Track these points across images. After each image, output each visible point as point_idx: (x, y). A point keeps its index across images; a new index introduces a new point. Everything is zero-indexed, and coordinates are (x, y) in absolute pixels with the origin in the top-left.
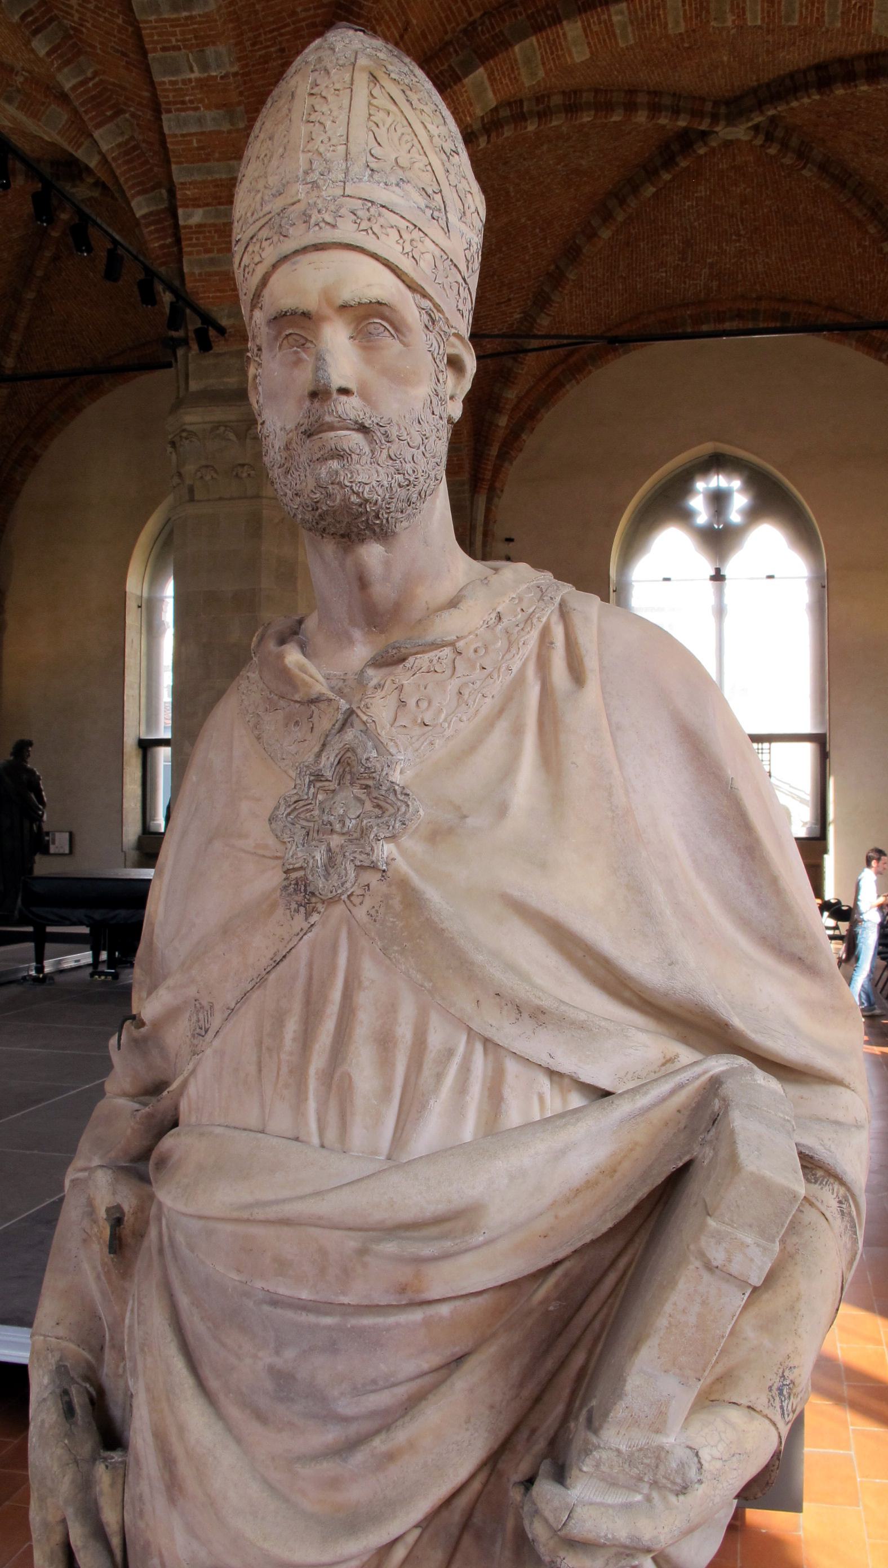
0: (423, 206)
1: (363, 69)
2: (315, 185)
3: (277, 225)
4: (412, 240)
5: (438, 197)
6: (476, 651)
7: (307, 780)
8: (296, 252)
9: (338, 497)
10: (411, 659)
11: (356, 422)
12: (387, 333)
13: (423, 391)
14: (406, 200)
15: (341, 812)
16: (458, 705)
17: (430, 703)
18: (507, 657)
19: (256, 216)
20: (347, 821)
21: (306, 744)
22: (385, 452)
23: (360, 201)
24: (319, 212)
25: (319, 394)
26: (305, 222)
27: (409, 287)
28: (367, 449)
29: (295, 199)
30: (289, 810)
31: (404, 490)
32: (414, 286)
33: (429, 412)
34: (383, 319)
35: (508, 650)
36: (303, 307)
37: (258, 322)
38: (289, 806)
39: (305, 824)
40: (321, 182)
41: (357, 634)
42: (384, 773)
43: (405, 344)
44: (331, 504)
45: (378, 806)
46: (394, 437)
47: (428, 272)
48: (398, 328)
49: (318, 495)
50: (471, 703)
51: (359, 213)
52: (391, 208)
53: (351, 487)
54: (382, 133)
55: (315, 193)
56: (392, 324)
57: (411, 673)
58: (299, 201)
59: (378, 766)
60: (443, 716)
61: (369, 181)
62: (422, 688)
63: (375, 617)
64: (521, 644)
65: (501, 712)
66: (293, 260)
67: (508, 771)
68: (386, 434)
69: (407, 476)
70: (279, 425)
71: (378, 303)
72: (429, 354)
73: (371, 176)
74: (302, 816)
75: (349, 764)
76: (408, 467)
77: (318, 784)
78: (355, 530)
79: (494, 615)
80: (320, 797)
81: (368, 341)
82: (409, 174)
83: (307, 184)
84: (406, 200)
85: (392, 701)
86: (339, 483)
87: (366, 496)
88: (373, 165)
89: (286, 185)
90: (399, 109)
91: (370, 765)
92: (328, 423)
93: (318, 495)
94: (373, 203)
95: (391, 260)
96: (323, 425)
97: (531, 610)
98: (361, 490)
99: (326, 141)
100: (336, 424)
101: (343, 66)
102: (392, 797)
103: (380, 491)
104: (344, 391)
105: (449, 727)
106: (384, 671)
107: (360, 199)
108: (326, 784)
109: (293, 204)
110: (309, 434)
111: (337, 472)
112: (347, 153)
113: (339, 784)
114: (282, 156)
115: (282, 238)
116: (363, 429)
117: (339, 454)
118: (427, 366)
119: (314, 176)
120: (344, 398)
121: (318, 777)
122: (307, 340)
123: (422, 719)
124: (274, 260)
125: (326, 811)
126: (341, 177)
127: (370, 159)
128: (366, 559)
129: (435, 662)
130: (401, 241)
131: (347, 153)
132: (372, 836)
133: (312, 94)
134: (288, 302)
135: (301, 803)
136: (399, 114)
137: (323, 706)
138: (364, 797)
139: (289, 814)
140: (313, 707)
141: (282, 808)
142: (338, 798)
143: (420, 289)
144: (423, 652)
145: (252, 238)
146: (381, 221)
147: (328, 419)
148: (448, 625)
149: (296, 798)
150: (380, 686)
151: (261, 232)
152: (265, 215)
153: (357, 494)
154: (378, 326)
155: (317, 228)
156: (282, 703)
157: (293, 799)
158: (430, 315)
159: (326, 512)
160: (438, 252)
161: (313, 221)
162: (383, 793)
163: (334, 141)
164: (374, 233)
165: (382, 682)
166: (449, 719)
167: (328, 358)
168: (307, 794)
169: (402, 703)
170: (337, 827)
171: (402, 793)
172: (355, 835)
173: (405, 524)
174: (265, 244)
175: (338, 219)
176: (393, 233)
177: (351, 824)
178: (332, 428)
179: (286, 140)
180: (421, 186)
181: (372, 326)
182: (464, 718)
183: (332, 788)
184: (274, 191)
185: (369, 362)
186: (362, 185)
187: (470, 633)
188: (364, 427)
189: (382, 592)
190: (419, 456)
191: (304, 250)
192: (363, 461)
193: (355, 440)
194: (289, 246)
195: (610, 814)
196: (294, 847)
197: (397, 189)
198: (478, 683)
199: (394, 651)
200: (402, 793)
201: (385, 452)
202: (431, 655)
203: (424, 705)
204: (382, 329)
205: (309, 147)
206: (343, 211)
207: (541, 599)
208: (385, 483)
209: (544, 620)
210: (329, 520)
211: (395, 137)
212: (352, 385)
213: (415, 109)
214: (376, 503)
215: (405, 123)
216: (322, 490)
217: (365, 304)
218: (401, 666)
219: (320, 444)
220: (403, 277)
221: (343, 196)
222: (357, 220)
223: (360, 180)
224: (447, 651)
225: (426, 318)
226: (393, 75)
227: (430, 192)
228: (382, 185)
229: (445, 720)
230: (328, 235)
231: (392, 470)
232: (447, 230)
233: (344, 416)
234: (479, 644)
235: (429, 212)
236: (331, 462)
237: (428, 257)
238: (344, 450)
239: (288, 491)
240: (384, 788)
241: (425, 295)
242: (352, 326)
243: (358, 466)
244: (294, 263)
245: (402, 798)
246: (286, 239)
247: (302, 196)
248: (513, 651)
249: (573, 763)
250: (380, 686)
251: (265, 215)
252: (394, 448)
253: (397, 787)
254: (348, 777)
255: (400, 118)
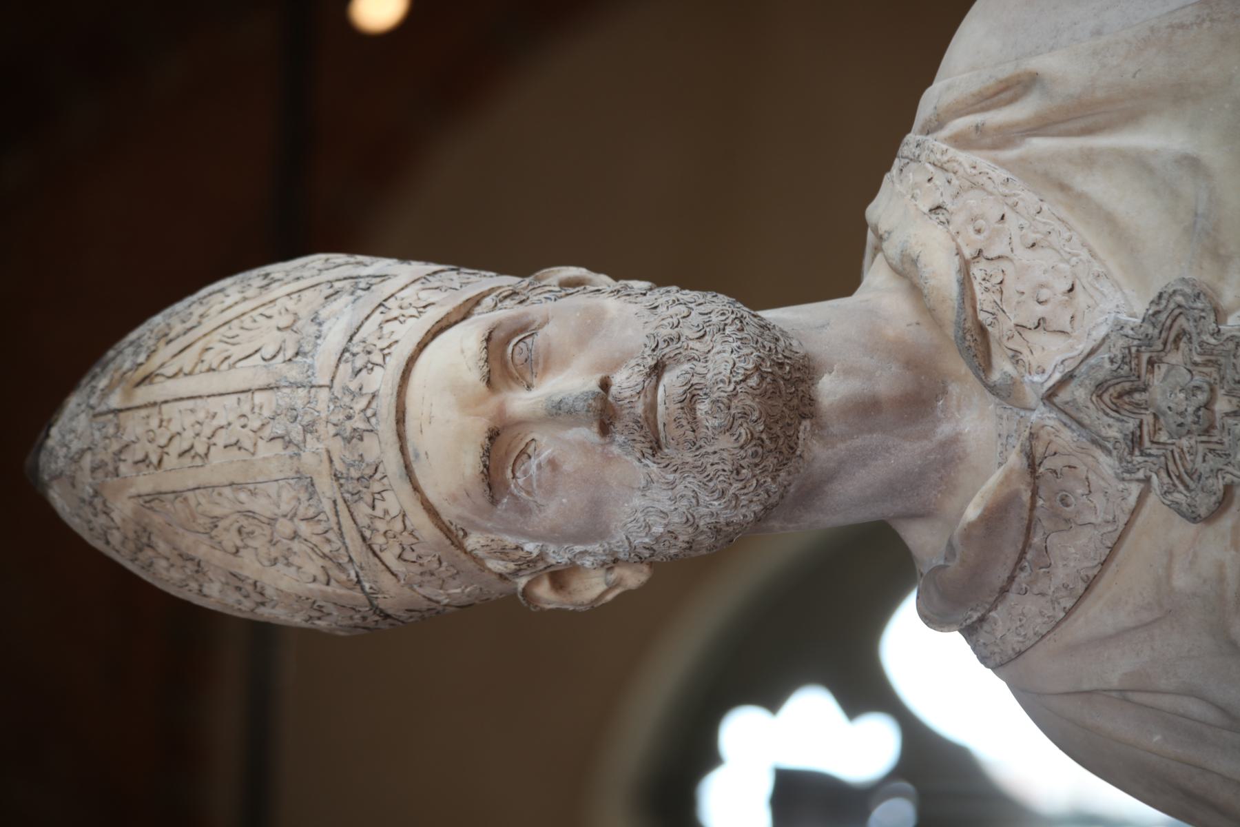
0: (352, 298)
1: (128, 395)
2: (308, 429)
3: (358, 482)
4: (401, 308)
5: (337, 285)
6: (979, 231)
7: (1140, 459)
8: (403, 450)
9: (749, 402)
10: (982, 316)
11: (649, 375)
12: (527, 340)
13: (612, 305)
14: (340, 318)
15: (1182, 396)
16: (1051, 247)
17: (1042, 286)
18: (990, 186)
19: (331, 535)
20: (1194, 383)
21: (1092, 477)
22: (691, 344)
23: (341, 366)
24: (349, 418)
25: (604, 413)
26: (361, 439)
27: (464, 319)
28: (686, 366)
29: (325, 457)
30: (1181, 488)
31: (746, 328)
32: (464, 311)
33: (641, 298)
34: (508, 343)
35: (982, 187)
36: (482, 438)
37: (483, 542)
38: (1174, 485)
39: (1199, 459)
40: (307, 419)
41: (945, 430)
42: (1131, 332)
43: (546, 322)
44: (757, 414)
45: (1177, 339)
46: (674, 332)
47: (444, 295)
48: (523, 329)
49: (743, 431)
50: (1048, 228)
51: (359, 362)
52: (353, 330)
53: (737, 383)
54: (237, 352)
55: (321, 428)
56: (516, 333)
57: (1000, 316)
58: (328, 452)
59: (1121, 342)
60: (1062, 266)
61: (312, 357)
62: (1023, 297)
63: (919, 401)
64: (974, 171)
65: (1063, 188)
66: (412, 458)
67: (1140, 164)
68: (669, 341)
69: (729, 321)
70: (638, 502)
71: (488, 339)
72: (559, 301)
73: (305, 354)
74: (1189, 466)
75: (1120, 396)
76: (715, 319)
77: (1147, 443)
78: (795, 402)
79: (934, 216)
80: (1163, 437)
81: (537, 364)
82: (305, 313)
83: (305, 441)
84: (340, 318)
85: (1038, 338)
86: (730, 398)
87: (751, 366)
88: (290, 353)
89: (299, 476)
90: (199, 339)
91: (1120, 356)
92: (645, 411)
93: (743, 431)
94: (345, 350)
95: (428, 327)
96: (647, 419)
97: (931, 168)
98: (742, 371)
99: (243, 421)
100: (648, 400)
101: (118, 427)
102: (1163, 317)
103: (745, 351)
104: (605, 385)
105: (1077, 255)
106: (994, 347)
107: (337, 366)
108: (1145, 429)
109: (331, 461)
110: (656, 447)
111: (713, 402)
112: (268, 388)
113: (1146, 409)
114: (253, 493)
115: (378, 476)
116: (658, 370)
117: (690, 398)
118: (579, 300)
119: (296, 432)
120: (614, 390)
121: (1135, 441)
122: (523, 452)
123: (1064, 294)
124: (408, 487)
125: (1180, 420)
126: (302, 392)
127: (280, 358)
128: (838, 396)
129: (988, 285)
130: (402, 319)
131: (268, 388)
132: (1212, 341)
133: (160, 461)
134: (471, 462)
135: (1172, 467)
136: (208, 338)
137: (1039, 450)
138: (1164, 368)
139: (1187, 487)
140: (1041, 470)
141: (1177, 497)
142: (1164, 406)
143: (469, 305)
144: (973, 299)
145: (364, 539)
146: (372, 339)
147: (640, 409)
148: (941, 271)
149: (1163, 474)
150: (1015, 357)
151: (359, 521)
152: (337, 515)
153: (746, 378)
154: (517, 349)
155: (373, 420)
156: (1037, 540)
157: (1166, 480)
158: (506, 297)
159: (768, 428)
160: (418, 286)
161: (362, 425)
162: (1157, 331)
163: (246, 408)
164: (389, 347)
165: (1011, 353)
166: (1067, 257)
167: (557, 399)
168: (1157, 456)
169: (1040, 324)
170: (1202, 397)
171: (1158, 304)
172: (1215, 375)
173: (795, 343)
174: (379, 512)
175: (364, 391)
176: (388, 327)
177: (1198, 380)
178: (652, 407)
179: (227, 491)
180: (323, 300)
181: (517, 357)
182: (1067, 235)
183: (1150, 419)
184: (304, 496)
185: (565, 363)
186: (317, 364)
187: (954, 240)
188: (656, 366)
189: (887, 381)
190: (703, 309)
191: (401, 436)
192: (704, 371)
193: (672, 381)
194: (392, 463)
195: (1207, 25)
196: (1230, 469)
197: (325, 328)
198: (1022, 221)
199: (968, 337)
200: (1158, 304)
201: (691, 344)
202: (978, 289)
203: (1044, 294)
204: (521, 344)
205: (247, 444)
206: (353, 386)
207: (917, 159)
208: (735, 345)
209: (944, 147)
210: (777, 429)
211: (244, 335)
212: (599, 376)
213: (200, 323)
214: (763, 360)
215: (226, 327)
216: (737, 423)
217: (488, 353)
218: (990, 329)
219: (673, 425)
220: (453, 320)
221: (330, 387)
222: (370, 367)
223: (311, 366)
224: (977, 271)
225: (508, 302)
226: (141, 358)
227: (331, 291)
228: (319, 341)
229: (1068, 262)
230: (386, 405)
231: (718, 337)
232: (384, 277)
233: (639, 388)
234: (971, 229)
235: (359, 293)
236: (698, 413)
237: (423, 295)
238: (685, 392)
239: (732, 490)
240: (1150, 331)
241: (477, 301)
242: (513, 384)
243: (709, 376)
244: (417, 456)
245: (1164, 302)
246: (381, 469)
247: (321, 446)
248: (983, 179)
249: (1134, 76)
250: (1015, 357)
251: (337, 515)
252: (687, 332)
253: (1151, 312)
254: (1137, 396)
255: (216, 336)
